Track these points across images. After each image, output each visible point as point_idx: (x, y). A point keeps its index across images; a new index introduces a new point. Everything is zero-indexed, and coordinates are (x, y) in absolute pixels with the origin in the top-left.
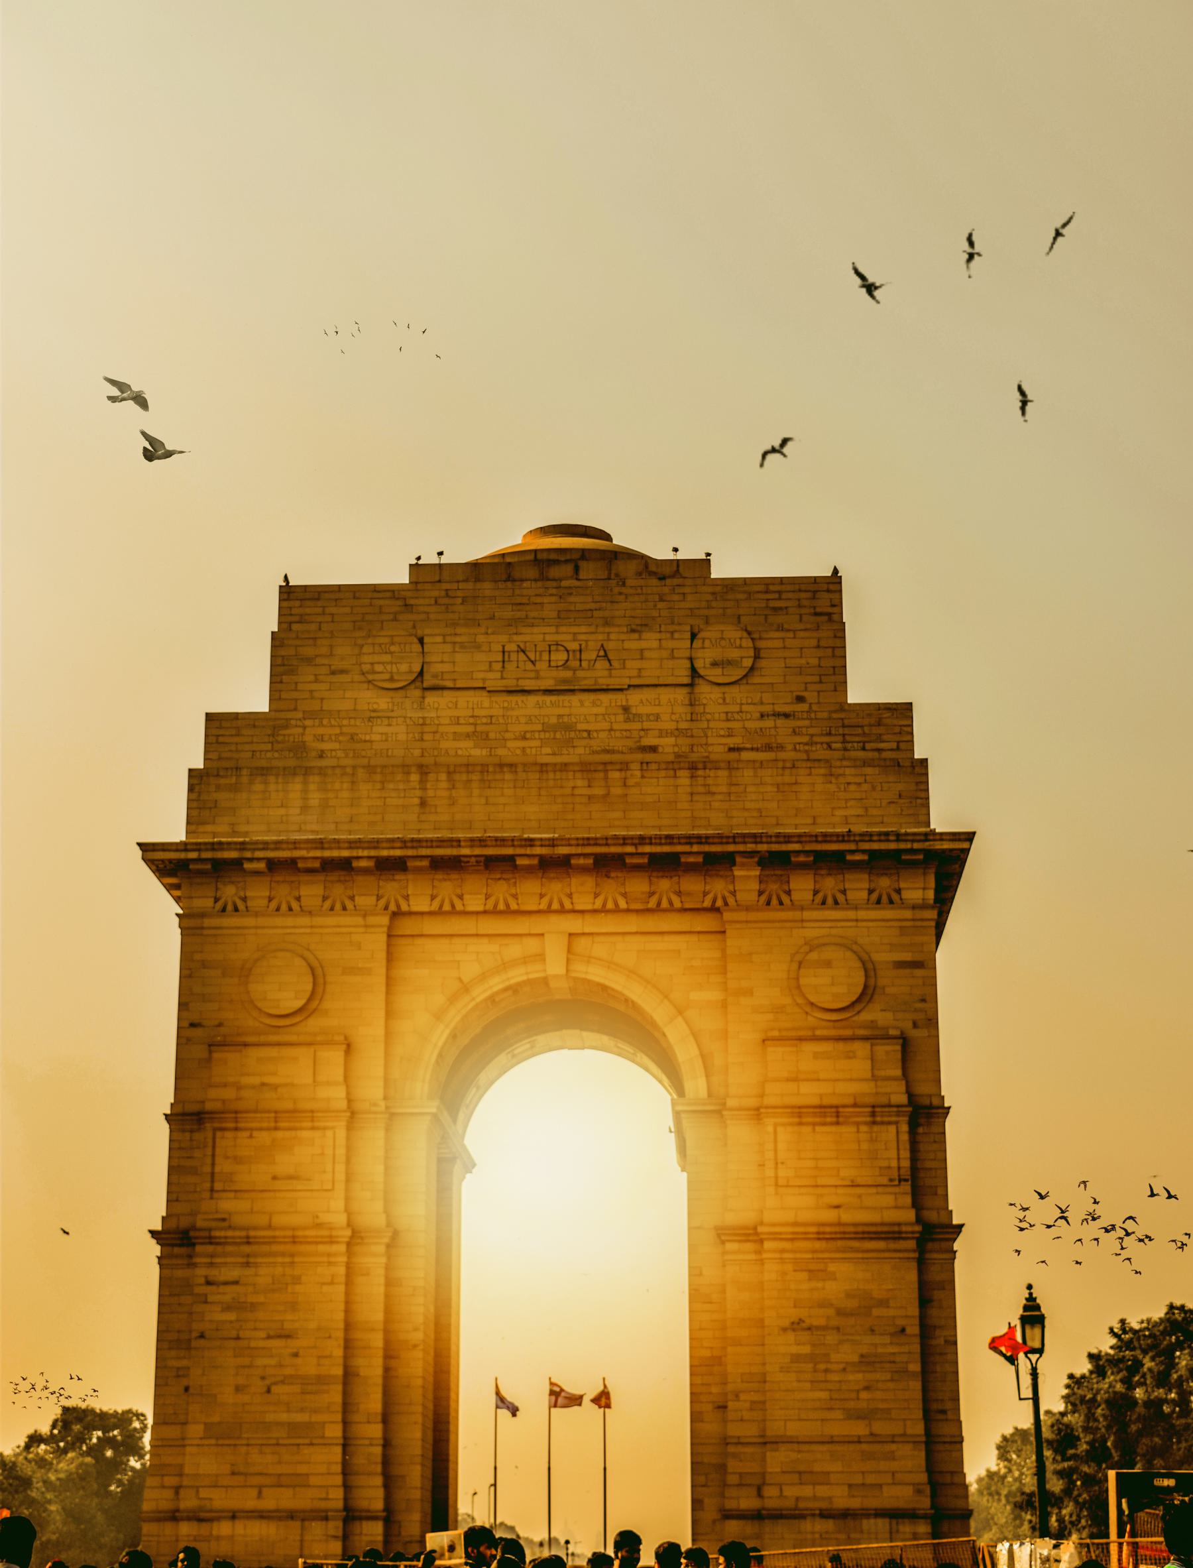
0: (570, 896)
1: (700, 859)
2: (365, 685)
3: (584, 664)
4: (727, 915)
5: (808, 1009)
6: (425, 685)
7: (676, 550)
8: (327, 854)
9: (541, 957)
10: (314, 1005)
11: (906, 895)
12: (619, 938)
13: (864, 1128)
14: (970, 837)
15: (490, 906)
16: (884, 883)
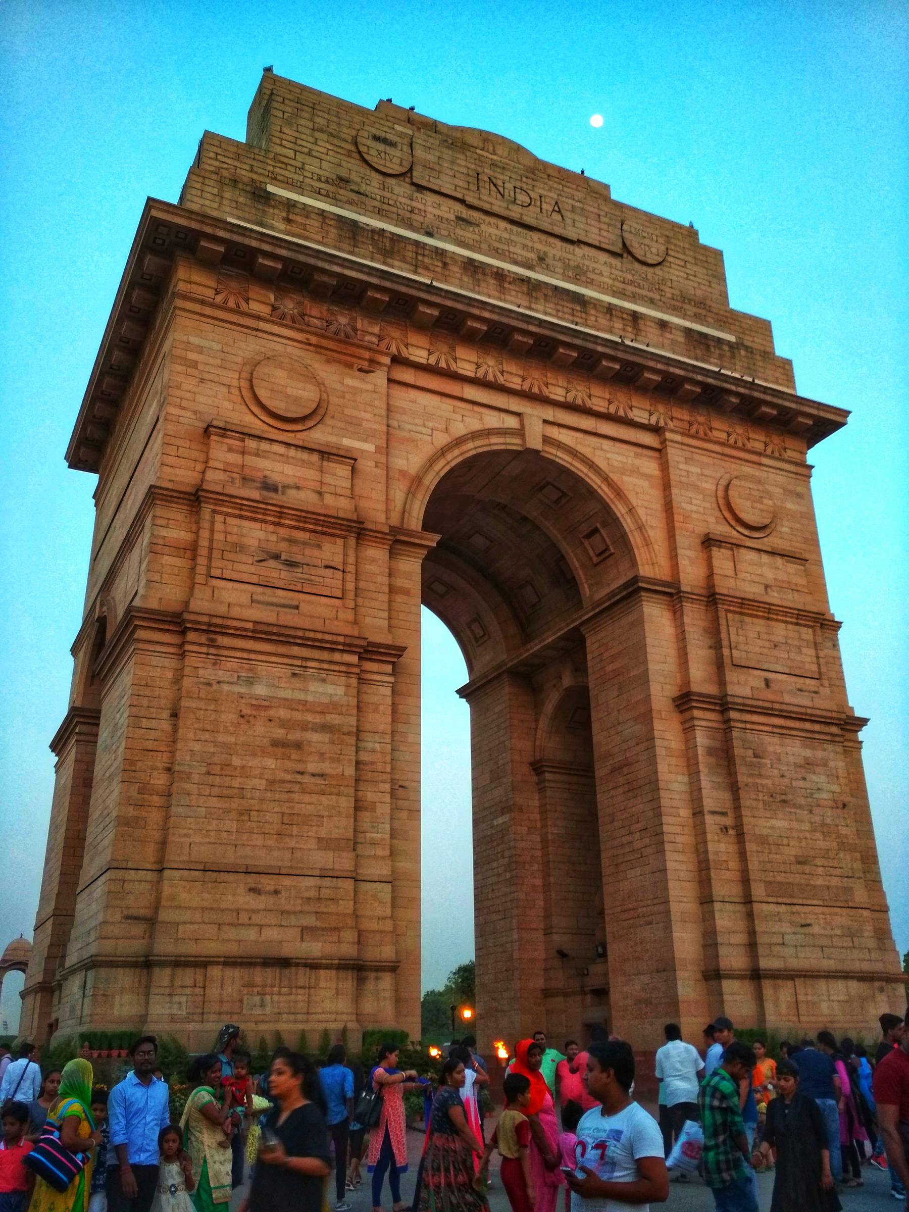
0: (547, 385)
1: (657, 378)
2: (360, 163)
3: (544, 211)
4: (668, 435)
5: (733, 523)
6: (415, 180)
7: (583, 172)
8: (347, 272)
9: (520, 432)
10: (318, 418)
11: (789, 454)
12: (579, 435)
13: (790, 627)
14: (846, 413)
15: (480, 374)
16: (776, 440)
